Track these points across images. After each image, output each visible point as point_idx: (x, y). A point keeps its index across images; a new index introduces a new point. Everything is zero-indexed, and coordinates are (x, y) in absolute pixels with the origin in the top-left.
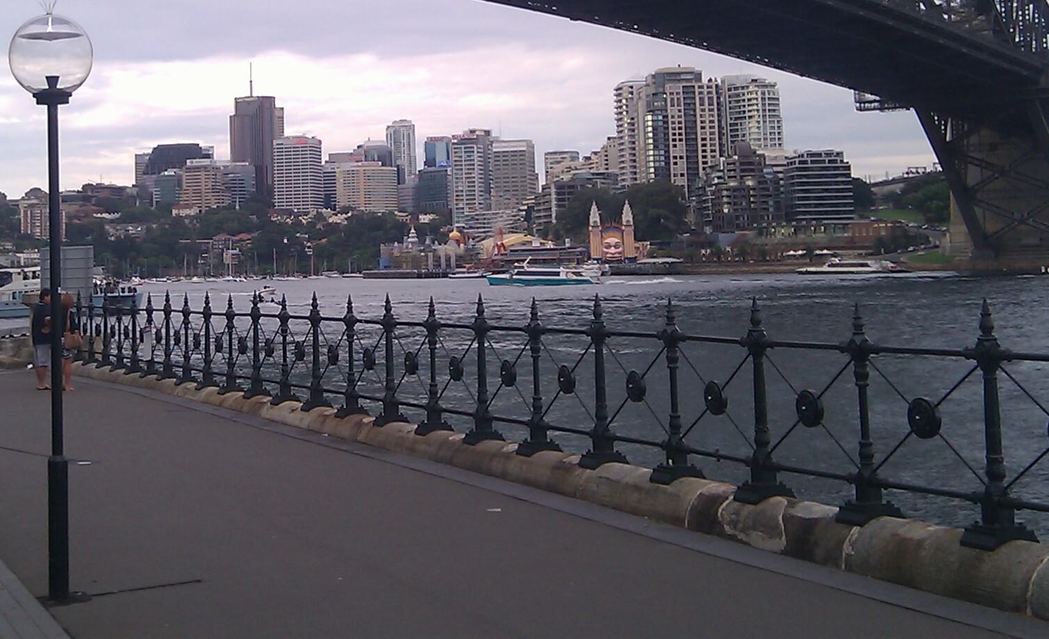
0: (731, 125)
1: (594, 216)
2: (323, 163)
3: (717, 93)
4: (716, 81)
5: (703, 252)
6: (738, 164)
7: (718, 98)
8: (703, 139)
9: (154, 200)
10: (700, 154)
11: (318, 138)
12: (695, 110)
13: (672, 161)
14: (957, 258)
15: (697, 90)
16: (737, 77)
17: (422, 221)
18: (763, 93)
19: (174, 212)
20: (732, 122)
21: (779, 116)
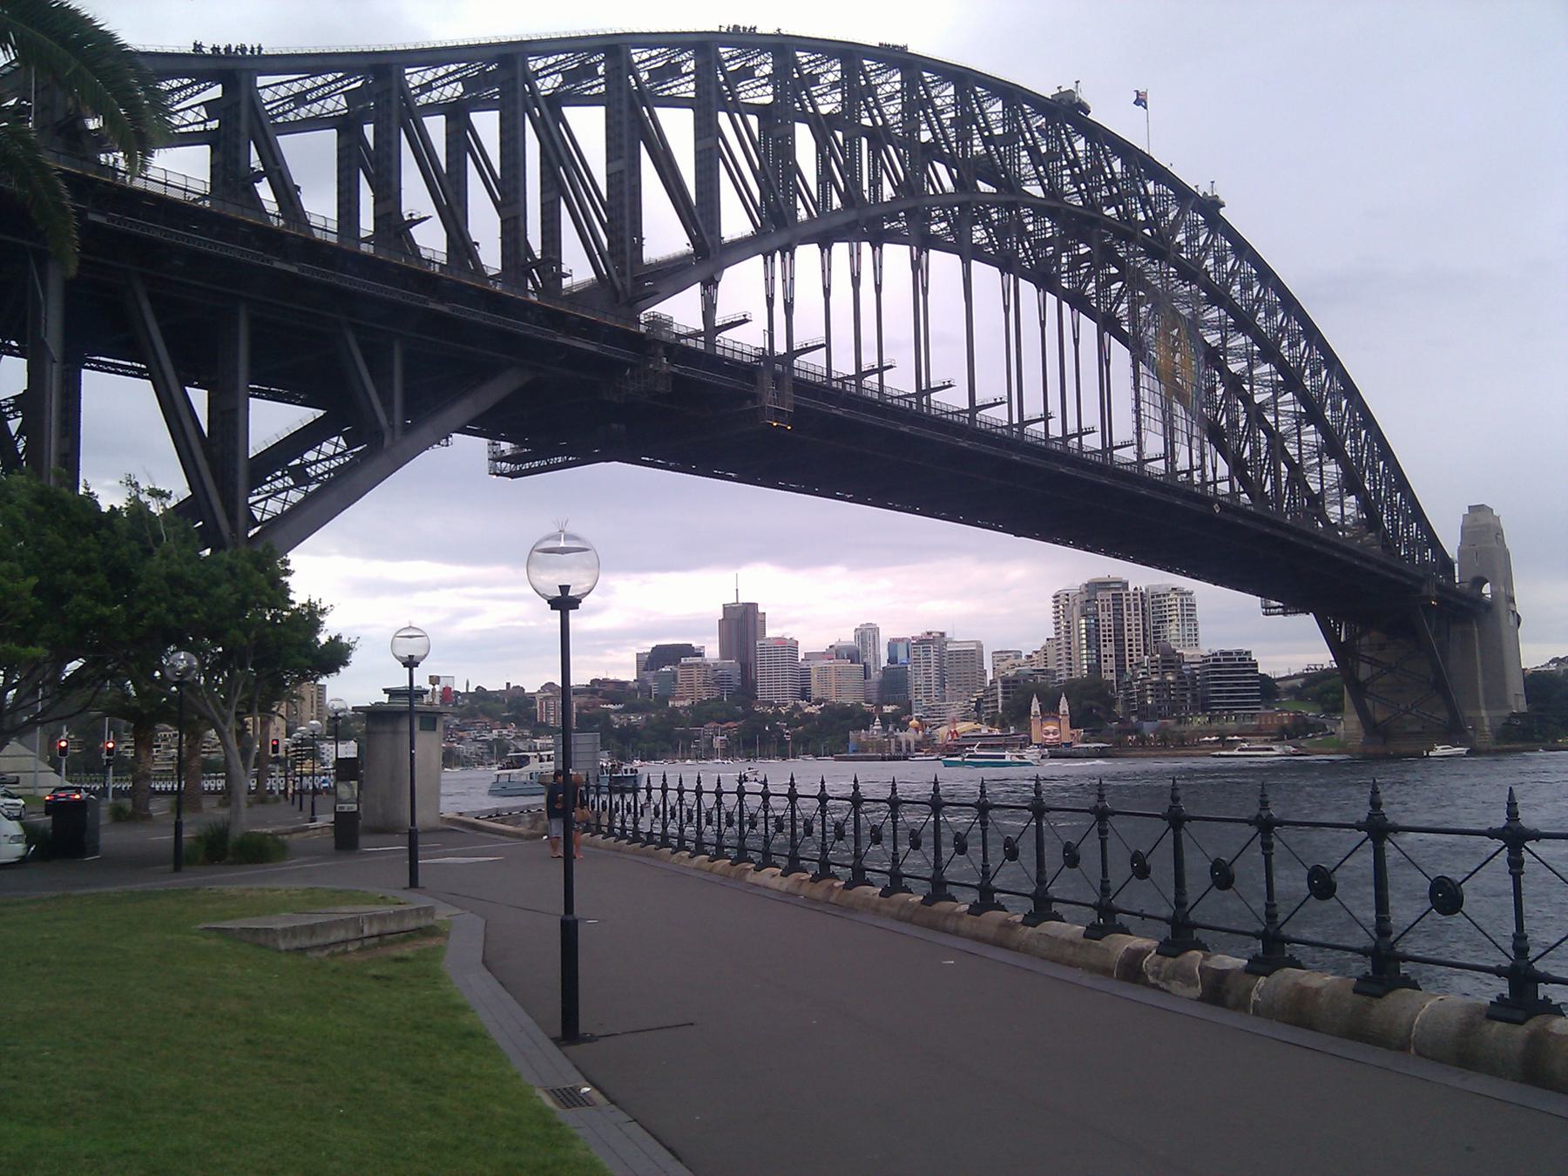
0: (1154, 628)
1: (1035, 707)
2: (800, 661)
3: (1142, 599)
4: (1141, 589)
5: (1130, 738)
6: (1160, 661)
7: (1143, 604)
8: (1130, 640)
9: (653, 693)
10: (1127, 653)
11: (795, 639)
12: (1122, 615)
13: (1103, 659)
14: (1350, 743)
15: (1124, 597)
16: (1160, 586)
17: (886, 711)
18: (1182, 600)
19: (670, 703)
20: (1155, 625)
21: (1195, 620)
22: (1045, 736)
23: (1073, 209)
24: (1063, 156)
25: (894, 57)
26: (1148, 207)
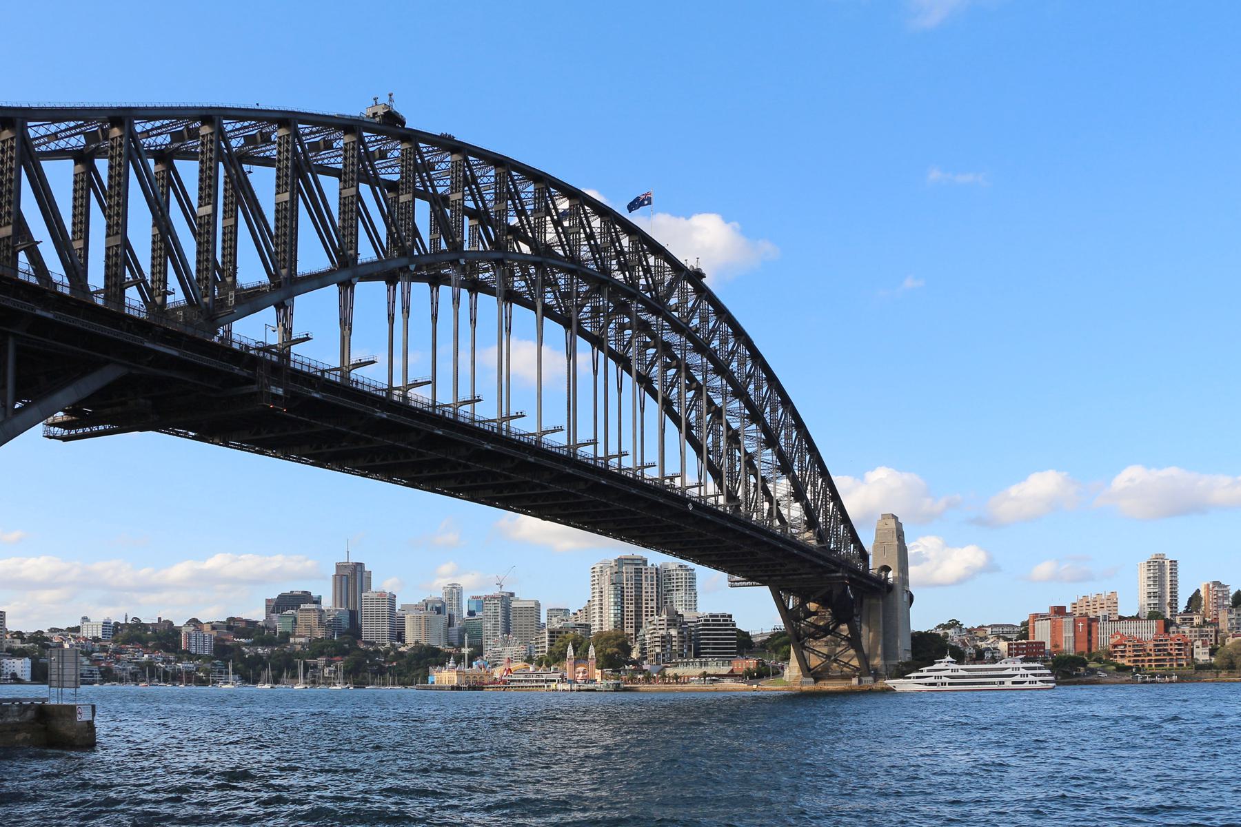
1: (570, 652)
7: (657, 577)
15: (643, 571)
19: (292, 640)
23: (587, 271)
24: (582, 230)
25: (447, 144)
26: (649, 275)
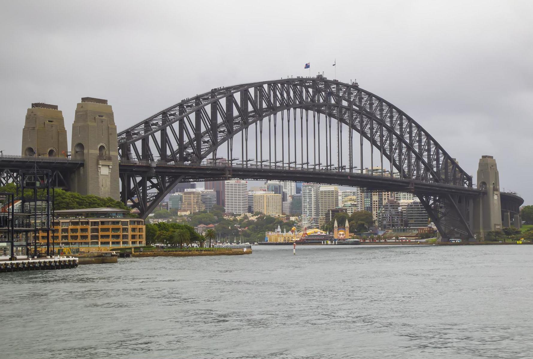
1: (336, 224)
9: (169, 207)
13: (373, 202)
17: (291, 220)
19: (179, 213)
22: (339, 236)
